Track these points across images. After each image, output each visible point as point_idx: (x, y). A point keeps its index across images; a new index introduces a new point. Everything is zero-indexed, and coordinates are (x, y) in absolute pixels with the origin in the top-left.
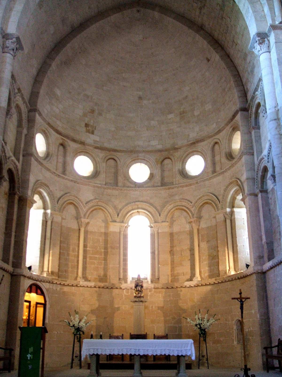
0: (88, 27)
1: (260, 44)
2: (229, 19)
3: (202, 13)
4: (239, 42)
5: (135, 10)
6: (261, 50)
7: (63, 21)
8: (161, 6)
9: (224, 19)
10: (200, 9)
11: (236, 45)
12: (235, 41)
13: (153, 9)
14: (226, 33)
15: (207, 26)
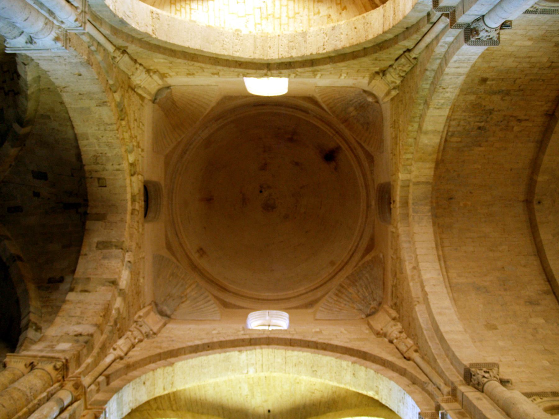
0: (551, 270)
1: (477, 33)
2: (516, 82)
3: (526, 118)
4: (545, 60)
5: (536, 207)
6: (484, 29)
7: (531, 302)
8: (533, 173)
9: (521, 88)
10: (520, 121)
11: (552, 62)
12: (549, 64)
13: (536, 182)
14: (543, 80)
15: (545, 108)
